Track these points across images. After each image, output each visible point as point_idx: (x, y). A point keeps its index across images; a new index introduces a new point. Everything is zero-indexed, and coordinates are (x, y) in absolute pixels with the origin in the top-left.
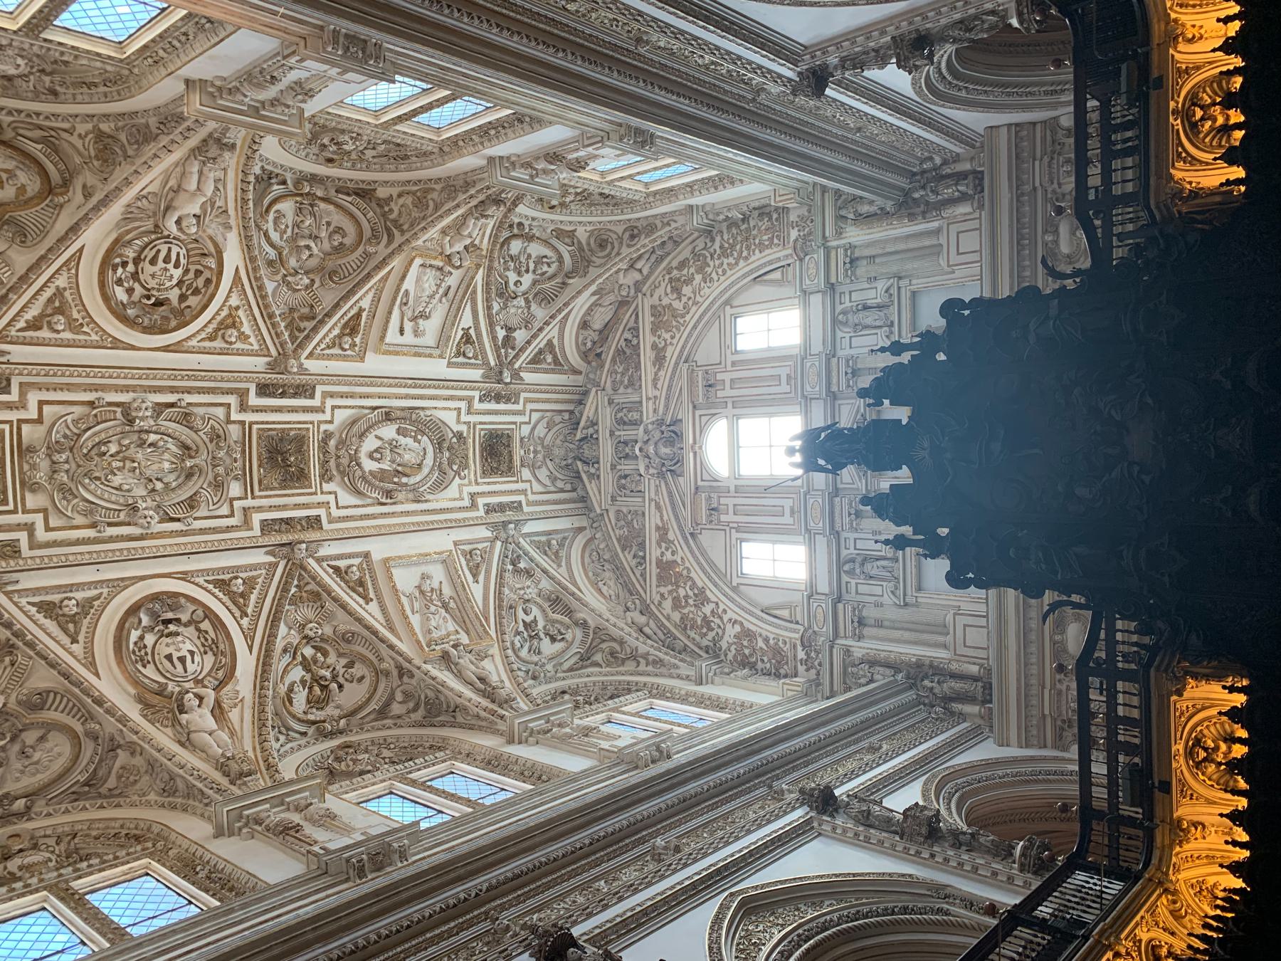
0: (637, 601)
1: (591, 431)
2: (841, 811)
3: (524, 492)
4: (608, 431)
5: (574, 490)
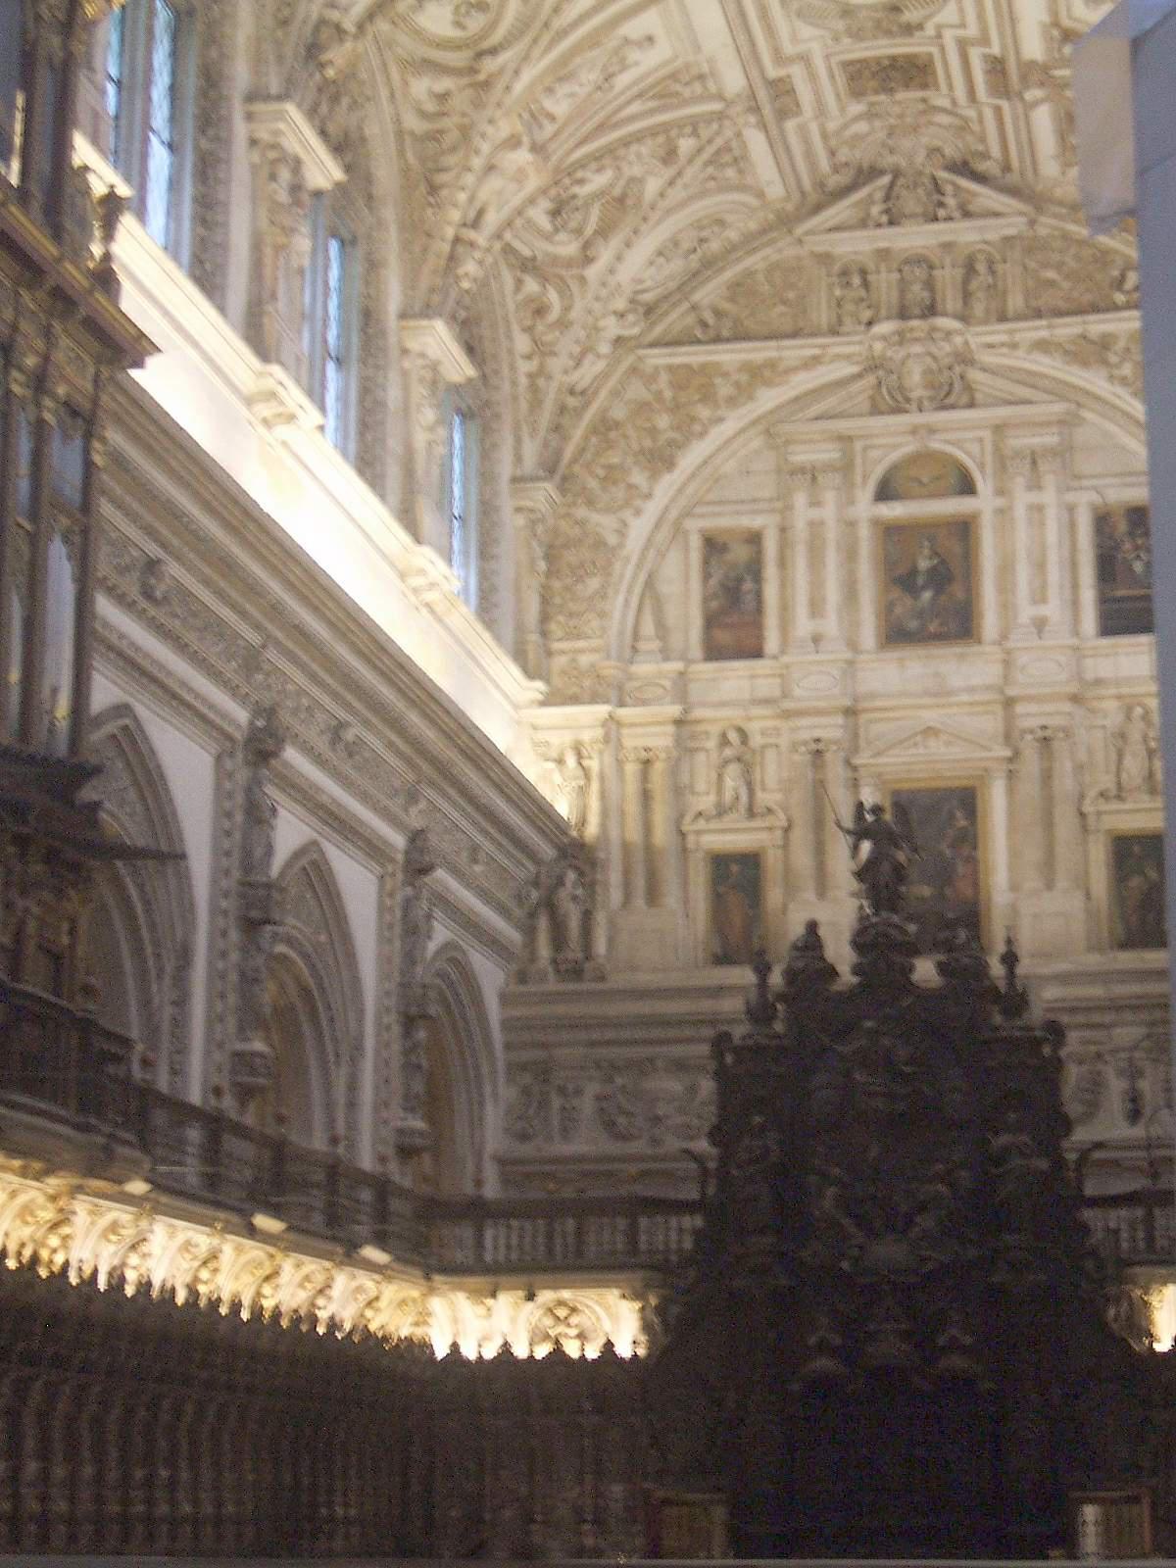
0: (635, 331)
1: (951, 201)
2: (409, 891)
3: (821, 111)
4: (947, 238)
5: (836, 170)
